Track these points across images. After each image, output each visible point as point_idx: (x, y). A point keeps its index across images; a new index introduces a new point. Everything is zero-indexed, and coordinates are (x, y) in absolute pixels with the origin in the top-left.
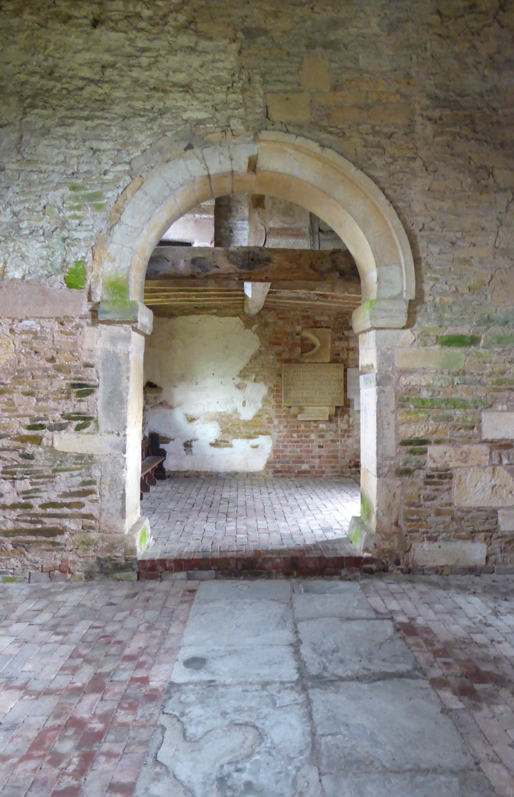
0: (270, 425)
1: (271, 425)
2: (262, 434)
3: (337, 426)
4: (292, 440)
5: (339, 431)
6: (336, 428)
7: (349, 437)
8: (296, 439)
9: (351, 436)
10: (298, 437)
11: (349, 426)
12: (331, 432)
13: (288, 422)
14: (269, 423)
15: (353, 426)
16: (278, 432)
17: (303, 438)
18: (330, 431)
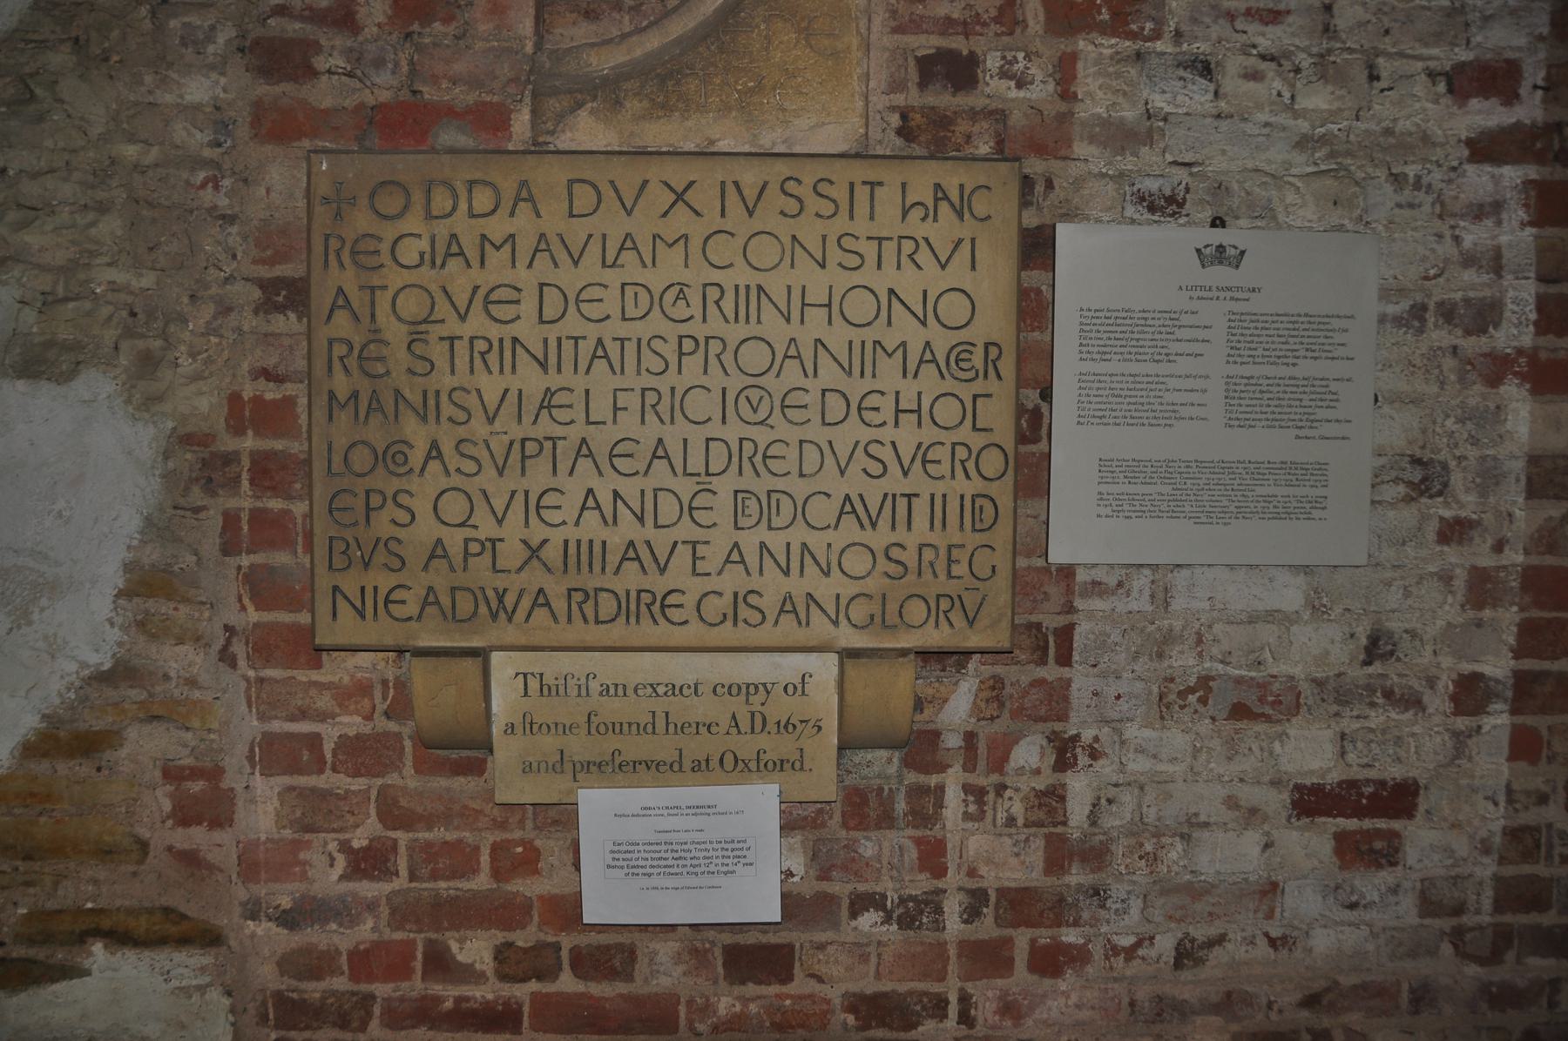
0: (198, 837)
1: (218, 845)
2: (120, 938)
3: (933, 857)
4: (449, 993)
5: (953, 907)
6: (921, 884)
7: (1049, 962)
8: (484, 993)
9: (1079, 956)
10: (510, 963)
11: (1058, 855)
12: (868, 920)
13: (393, 814)
14: (185, 816)
15: (1096, 856)
16: (288, 920)
17: (567, 983)
18: (860, 904)
